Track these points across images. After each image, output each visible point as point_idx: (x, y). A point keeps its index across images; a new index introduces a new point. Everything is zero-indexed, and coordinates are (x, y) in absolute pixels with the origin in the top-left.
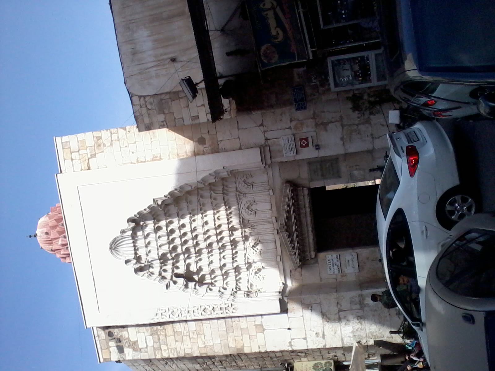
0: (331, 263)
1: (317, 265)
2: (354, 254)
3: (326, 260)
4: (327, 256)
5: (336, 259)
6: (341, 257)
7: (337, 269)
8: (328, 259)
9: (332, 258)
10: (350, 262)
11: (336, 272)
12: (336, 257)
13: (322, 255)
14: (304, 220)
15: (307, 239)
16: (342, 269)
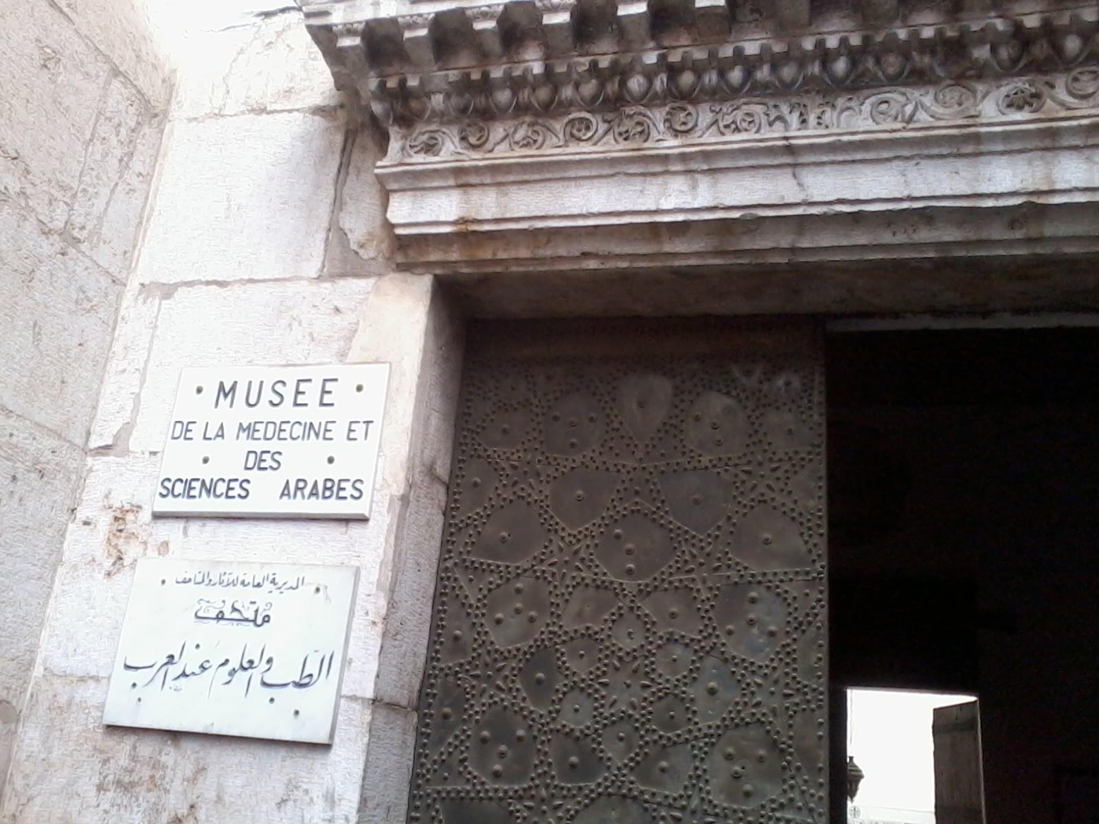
0: (287, 411)
1: (313, 267)
2: (311, 715)
3: (342, 355)
4: (376, 377)
5: (317, 473)
6: (334, 531)
7: (207, 474)
8: (349, 376)
9: (339, 431)
10: (236, 641)
11: (183, 461)
12: (335, 473)
13: (402, 318)
14: (858, 119)
15: (612, 147)
16: (194, 527)
